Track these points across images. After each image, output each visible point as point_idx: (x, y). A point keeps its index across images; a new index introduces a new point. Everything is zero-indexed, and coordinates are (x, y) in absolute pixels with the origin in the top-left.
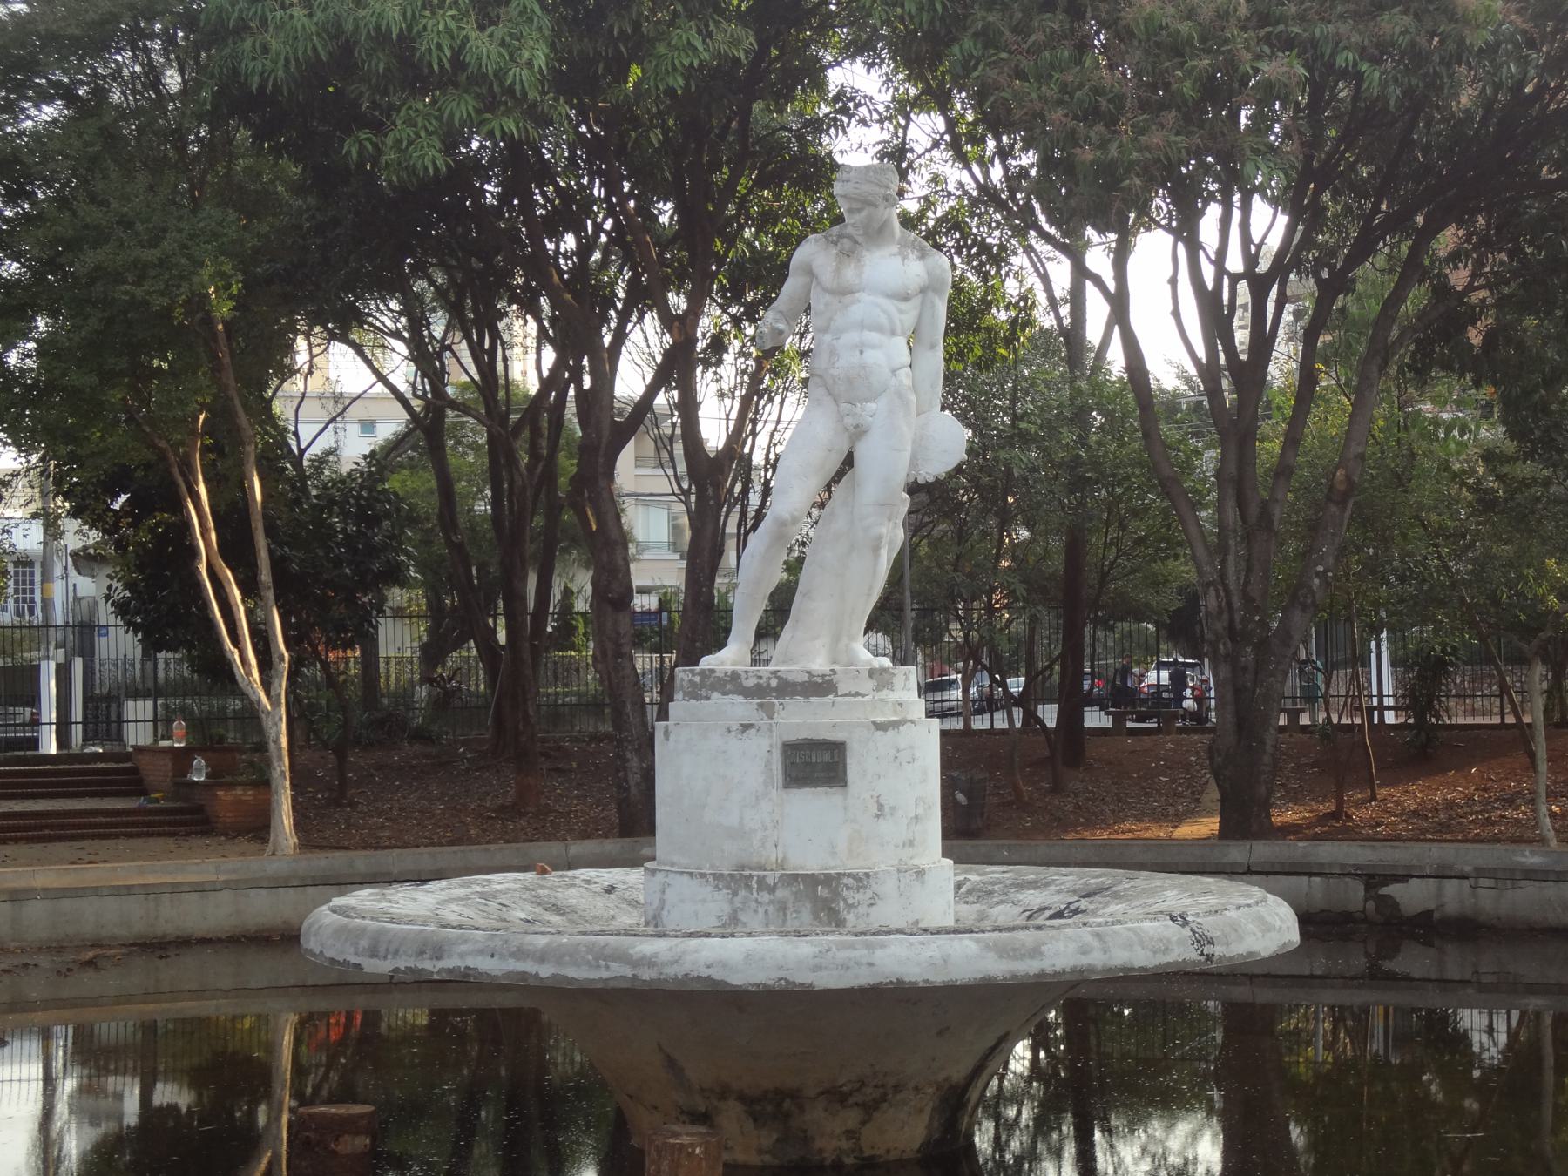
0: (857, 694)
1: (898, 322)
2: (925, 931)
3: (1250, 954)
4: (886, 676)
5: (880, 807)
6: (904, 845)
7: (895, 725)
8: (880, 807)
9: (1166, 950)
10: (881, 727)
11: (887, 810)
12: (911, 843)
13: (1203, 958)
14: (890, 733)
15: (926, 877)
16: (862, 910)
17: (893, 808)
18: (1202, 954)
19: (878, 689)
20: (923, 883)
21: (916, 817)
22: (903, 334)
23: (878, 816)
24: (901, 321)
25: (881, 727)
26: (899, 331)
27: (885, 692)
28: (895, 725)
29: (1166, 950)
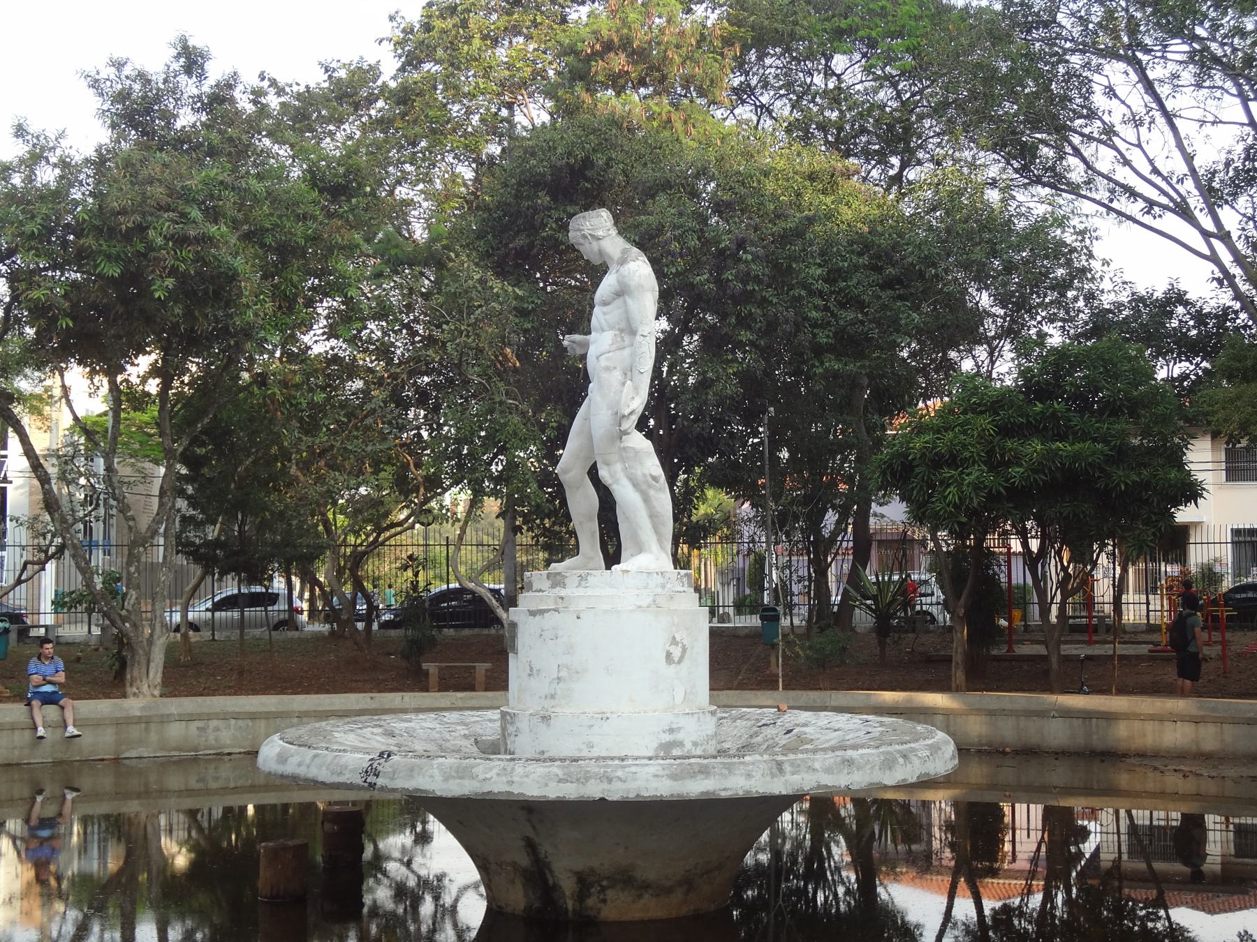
0: (540, 591)
1: (603, 321)
2: (552, 760)
3: (417, 790)
4: (558, 578)
5: (531, 669)
6: (546, 697)
7: (542, 612)
8: (531, 669)
9: (341, 773)
10: (533, 613)
11: (535, 671)
12: (553, 697)
13: (366, 785)
14: (538, 617)
15: (552, 721)
16: (512, 738)
17: (539, 671)
18: (365, 781)
19: (553, 586)
20: (549, 725)
21: (559, 678)
22: (612, 328)
23: (530, 675)
24: (606, 320)
25: (533, 613)
26: (605, 327)
27: (558, 588)
28: (542, 612)
29: (341, 773)
